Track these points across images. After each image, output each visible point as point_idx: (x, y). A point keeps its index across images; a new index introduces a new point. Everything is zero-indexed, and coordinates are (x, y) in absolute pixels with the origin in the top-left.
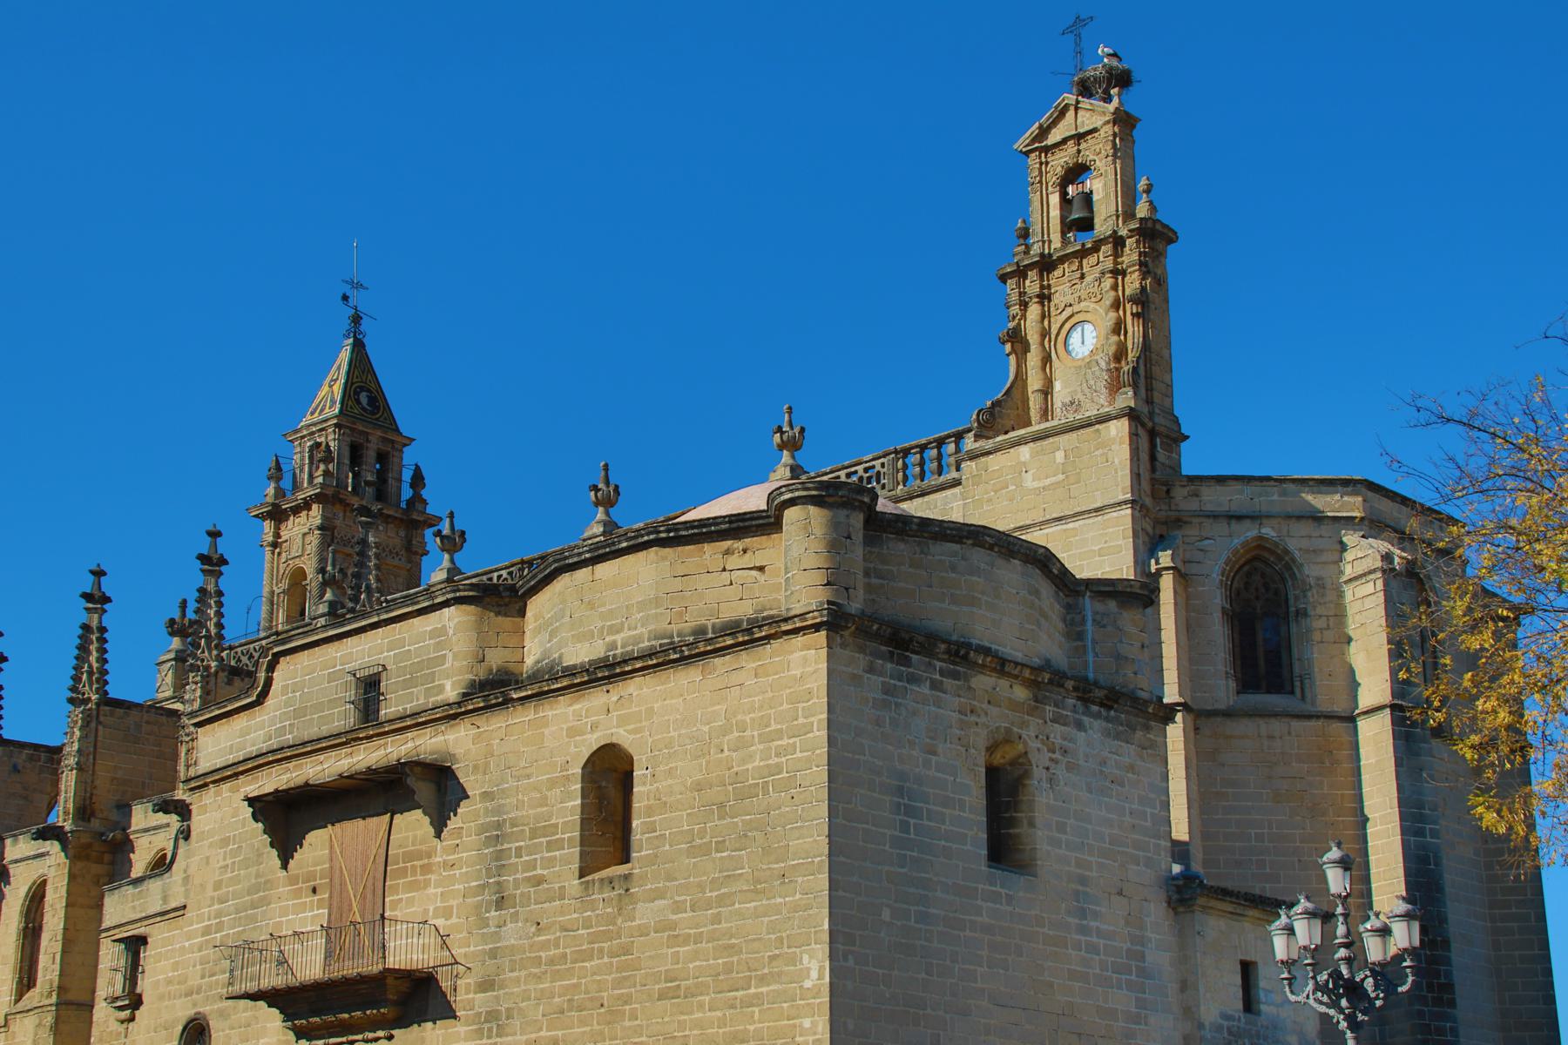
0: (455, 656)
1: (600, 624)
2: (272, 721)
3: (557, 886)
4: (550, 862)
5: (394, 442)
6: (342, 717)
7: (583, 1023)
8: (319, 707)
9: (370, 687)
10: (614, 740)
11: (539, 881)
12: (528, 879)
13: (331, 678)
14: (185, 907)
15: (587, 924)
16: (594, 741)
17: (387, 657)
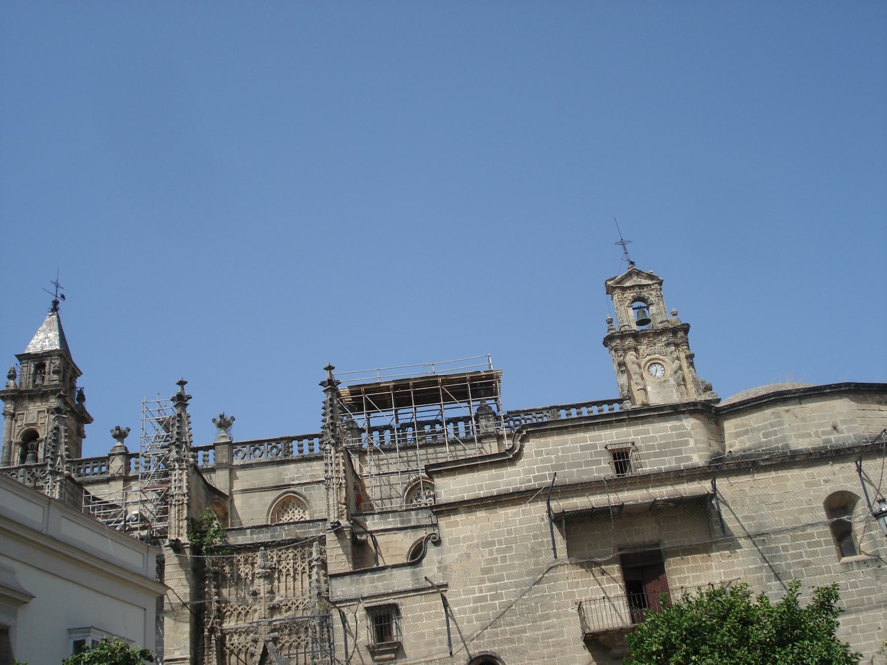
0: (696, 442)
1: (814, 430)
2: (530, 471)
3: (823, 566)
4: (815, 553)
5: (76, 373)
6: (605, 469)
7: (866, 638)
8: (578, 465)
9: (621, 458)
10: (844, 489)
11: (807, 564)
12: (798, 563)
13: (583, 448)
14: (446, 586)
15: (854, 585)
16: (828, 489)
17: (638, 439)
